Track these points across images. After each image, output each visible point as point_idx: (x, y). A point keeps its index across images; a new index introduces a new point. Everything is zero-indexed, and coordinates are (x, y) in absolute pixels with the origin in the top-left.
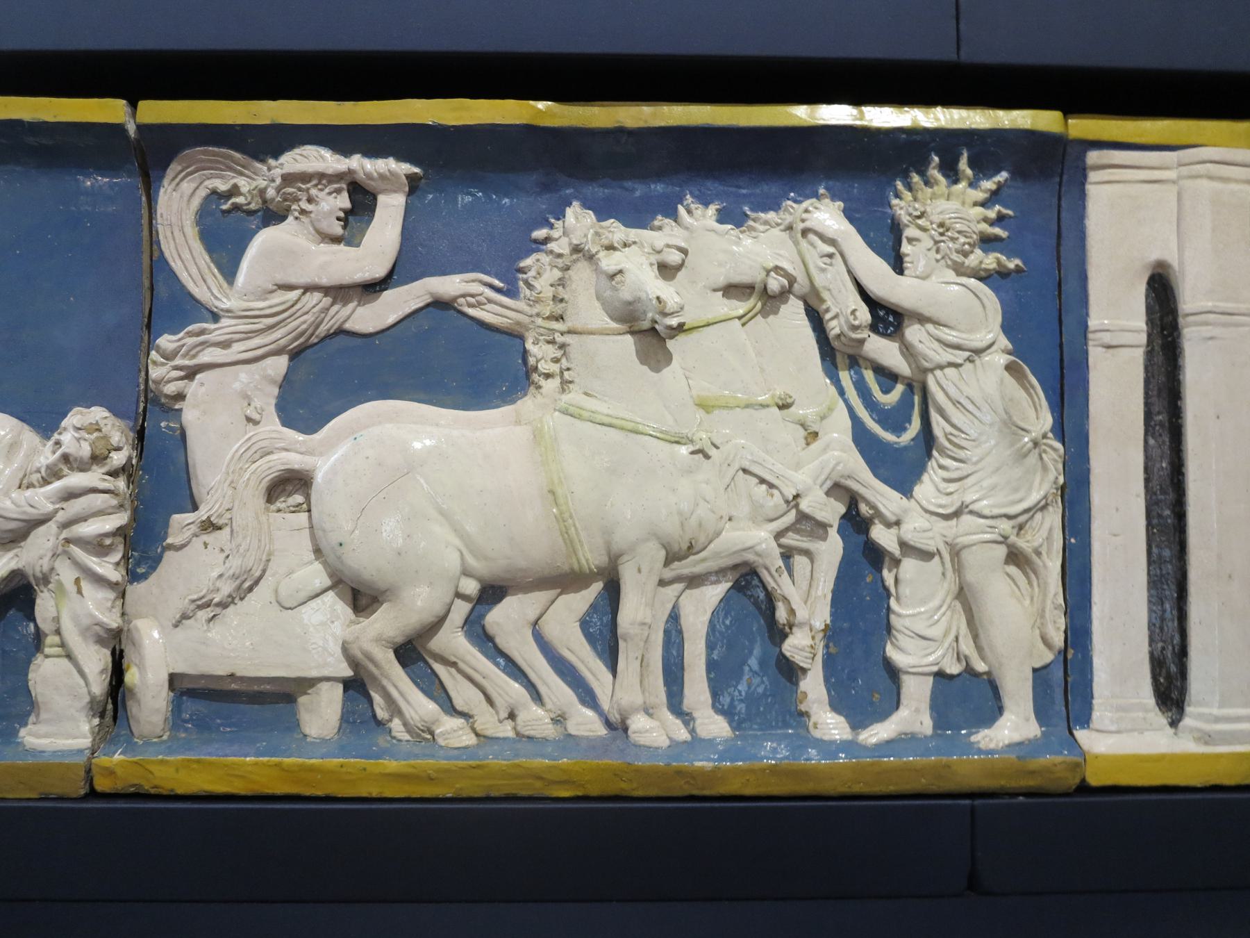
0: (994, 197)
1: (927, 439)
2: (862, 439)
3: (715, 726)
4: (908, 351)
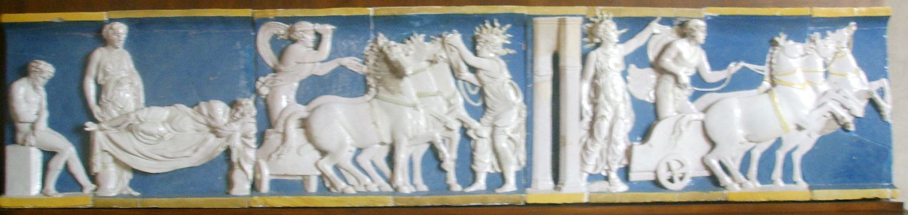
0: (508, 32)
1: (485, 106)
2: (468, 107)
3: (424, 188)
4: (478, 79)
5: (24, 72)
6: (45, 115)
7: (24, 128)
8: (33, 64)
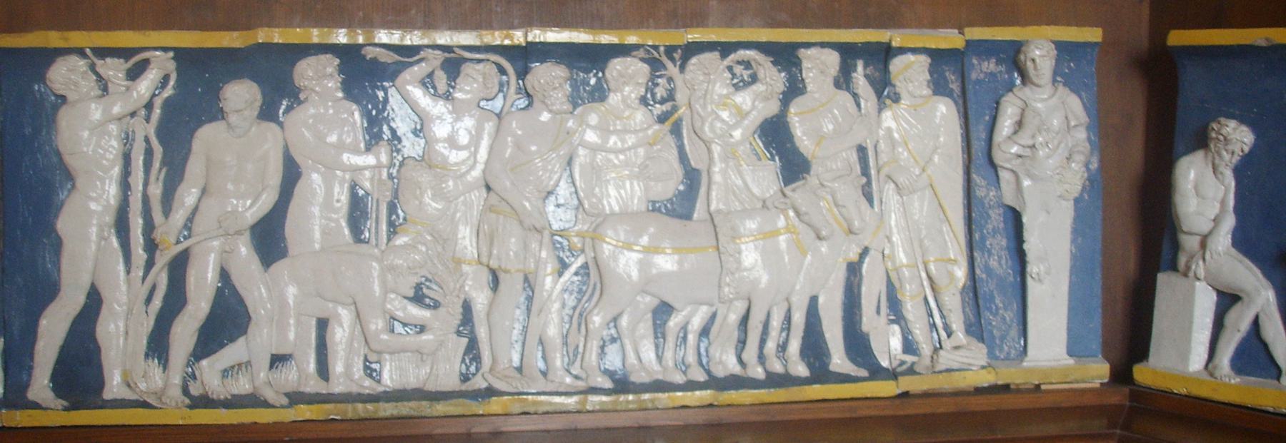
5: (1201, 141)
6: (1230, 222)
7: (1190, 243)
8: (1215, 126)
